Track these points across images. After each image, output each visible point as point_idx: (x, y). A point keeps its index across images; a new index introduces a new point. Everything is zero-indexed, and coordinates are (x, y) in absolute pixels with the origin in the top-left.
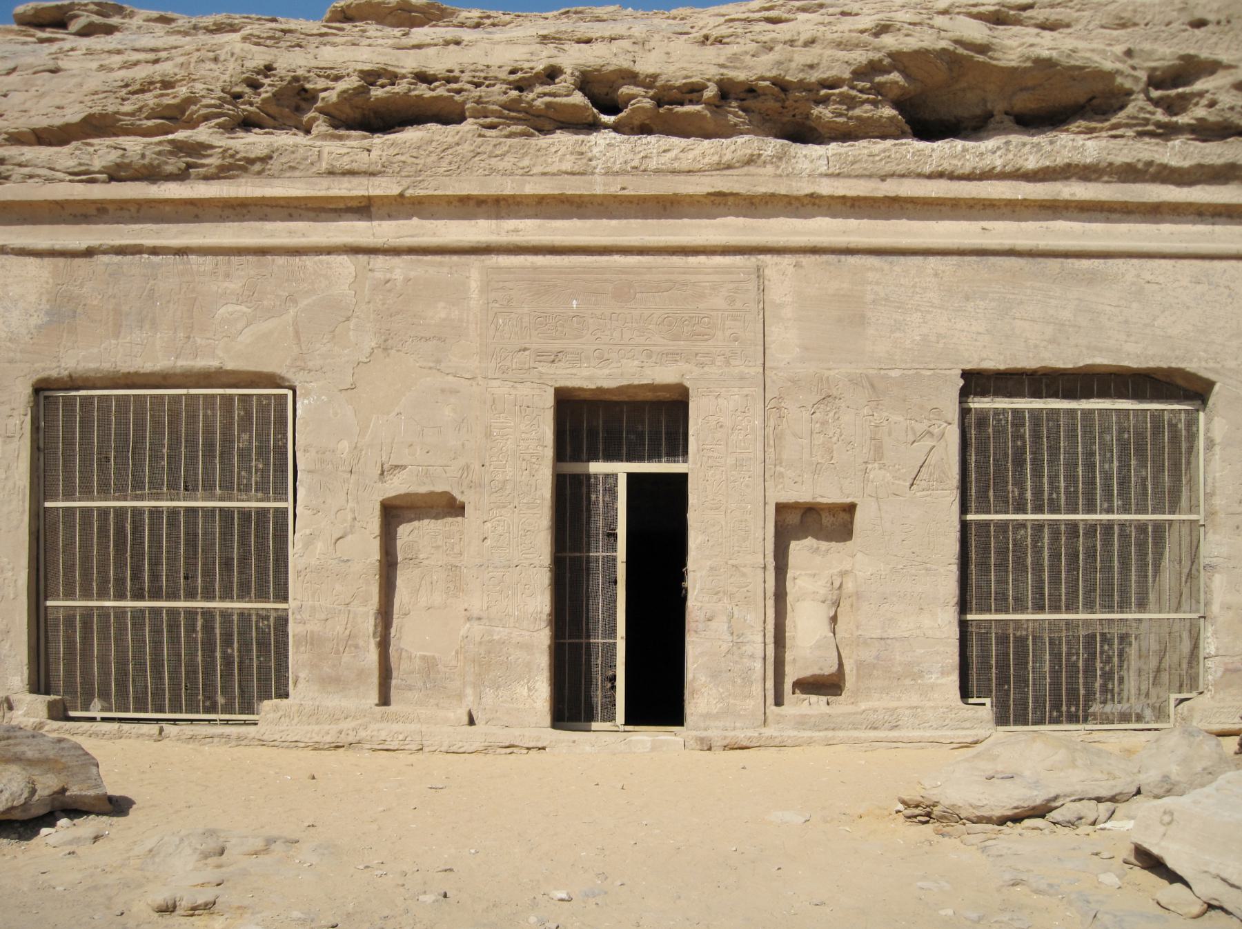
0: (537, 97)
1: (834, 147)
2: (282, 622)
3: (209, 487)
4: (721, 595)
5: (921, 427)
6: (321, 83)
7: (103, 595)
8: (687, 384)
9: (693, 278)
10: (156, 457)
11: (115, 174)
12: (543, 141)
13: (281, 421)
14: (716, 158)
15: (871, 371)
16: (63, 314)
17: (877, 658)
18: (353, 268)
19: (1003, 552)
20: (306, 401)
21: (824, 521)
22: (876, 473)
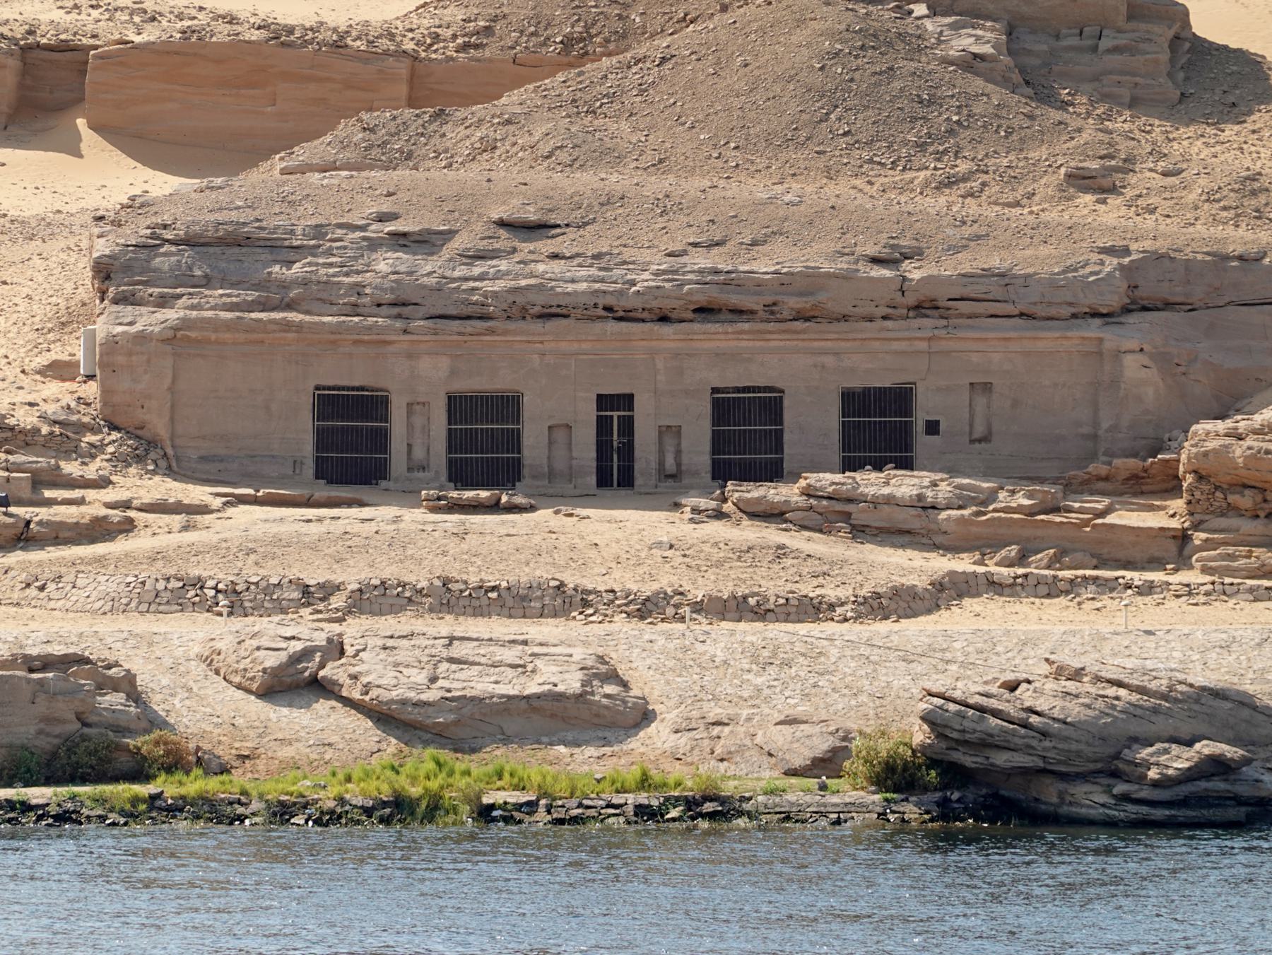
0: (592, 312)
2: (519, 459)
16: (453, 373)
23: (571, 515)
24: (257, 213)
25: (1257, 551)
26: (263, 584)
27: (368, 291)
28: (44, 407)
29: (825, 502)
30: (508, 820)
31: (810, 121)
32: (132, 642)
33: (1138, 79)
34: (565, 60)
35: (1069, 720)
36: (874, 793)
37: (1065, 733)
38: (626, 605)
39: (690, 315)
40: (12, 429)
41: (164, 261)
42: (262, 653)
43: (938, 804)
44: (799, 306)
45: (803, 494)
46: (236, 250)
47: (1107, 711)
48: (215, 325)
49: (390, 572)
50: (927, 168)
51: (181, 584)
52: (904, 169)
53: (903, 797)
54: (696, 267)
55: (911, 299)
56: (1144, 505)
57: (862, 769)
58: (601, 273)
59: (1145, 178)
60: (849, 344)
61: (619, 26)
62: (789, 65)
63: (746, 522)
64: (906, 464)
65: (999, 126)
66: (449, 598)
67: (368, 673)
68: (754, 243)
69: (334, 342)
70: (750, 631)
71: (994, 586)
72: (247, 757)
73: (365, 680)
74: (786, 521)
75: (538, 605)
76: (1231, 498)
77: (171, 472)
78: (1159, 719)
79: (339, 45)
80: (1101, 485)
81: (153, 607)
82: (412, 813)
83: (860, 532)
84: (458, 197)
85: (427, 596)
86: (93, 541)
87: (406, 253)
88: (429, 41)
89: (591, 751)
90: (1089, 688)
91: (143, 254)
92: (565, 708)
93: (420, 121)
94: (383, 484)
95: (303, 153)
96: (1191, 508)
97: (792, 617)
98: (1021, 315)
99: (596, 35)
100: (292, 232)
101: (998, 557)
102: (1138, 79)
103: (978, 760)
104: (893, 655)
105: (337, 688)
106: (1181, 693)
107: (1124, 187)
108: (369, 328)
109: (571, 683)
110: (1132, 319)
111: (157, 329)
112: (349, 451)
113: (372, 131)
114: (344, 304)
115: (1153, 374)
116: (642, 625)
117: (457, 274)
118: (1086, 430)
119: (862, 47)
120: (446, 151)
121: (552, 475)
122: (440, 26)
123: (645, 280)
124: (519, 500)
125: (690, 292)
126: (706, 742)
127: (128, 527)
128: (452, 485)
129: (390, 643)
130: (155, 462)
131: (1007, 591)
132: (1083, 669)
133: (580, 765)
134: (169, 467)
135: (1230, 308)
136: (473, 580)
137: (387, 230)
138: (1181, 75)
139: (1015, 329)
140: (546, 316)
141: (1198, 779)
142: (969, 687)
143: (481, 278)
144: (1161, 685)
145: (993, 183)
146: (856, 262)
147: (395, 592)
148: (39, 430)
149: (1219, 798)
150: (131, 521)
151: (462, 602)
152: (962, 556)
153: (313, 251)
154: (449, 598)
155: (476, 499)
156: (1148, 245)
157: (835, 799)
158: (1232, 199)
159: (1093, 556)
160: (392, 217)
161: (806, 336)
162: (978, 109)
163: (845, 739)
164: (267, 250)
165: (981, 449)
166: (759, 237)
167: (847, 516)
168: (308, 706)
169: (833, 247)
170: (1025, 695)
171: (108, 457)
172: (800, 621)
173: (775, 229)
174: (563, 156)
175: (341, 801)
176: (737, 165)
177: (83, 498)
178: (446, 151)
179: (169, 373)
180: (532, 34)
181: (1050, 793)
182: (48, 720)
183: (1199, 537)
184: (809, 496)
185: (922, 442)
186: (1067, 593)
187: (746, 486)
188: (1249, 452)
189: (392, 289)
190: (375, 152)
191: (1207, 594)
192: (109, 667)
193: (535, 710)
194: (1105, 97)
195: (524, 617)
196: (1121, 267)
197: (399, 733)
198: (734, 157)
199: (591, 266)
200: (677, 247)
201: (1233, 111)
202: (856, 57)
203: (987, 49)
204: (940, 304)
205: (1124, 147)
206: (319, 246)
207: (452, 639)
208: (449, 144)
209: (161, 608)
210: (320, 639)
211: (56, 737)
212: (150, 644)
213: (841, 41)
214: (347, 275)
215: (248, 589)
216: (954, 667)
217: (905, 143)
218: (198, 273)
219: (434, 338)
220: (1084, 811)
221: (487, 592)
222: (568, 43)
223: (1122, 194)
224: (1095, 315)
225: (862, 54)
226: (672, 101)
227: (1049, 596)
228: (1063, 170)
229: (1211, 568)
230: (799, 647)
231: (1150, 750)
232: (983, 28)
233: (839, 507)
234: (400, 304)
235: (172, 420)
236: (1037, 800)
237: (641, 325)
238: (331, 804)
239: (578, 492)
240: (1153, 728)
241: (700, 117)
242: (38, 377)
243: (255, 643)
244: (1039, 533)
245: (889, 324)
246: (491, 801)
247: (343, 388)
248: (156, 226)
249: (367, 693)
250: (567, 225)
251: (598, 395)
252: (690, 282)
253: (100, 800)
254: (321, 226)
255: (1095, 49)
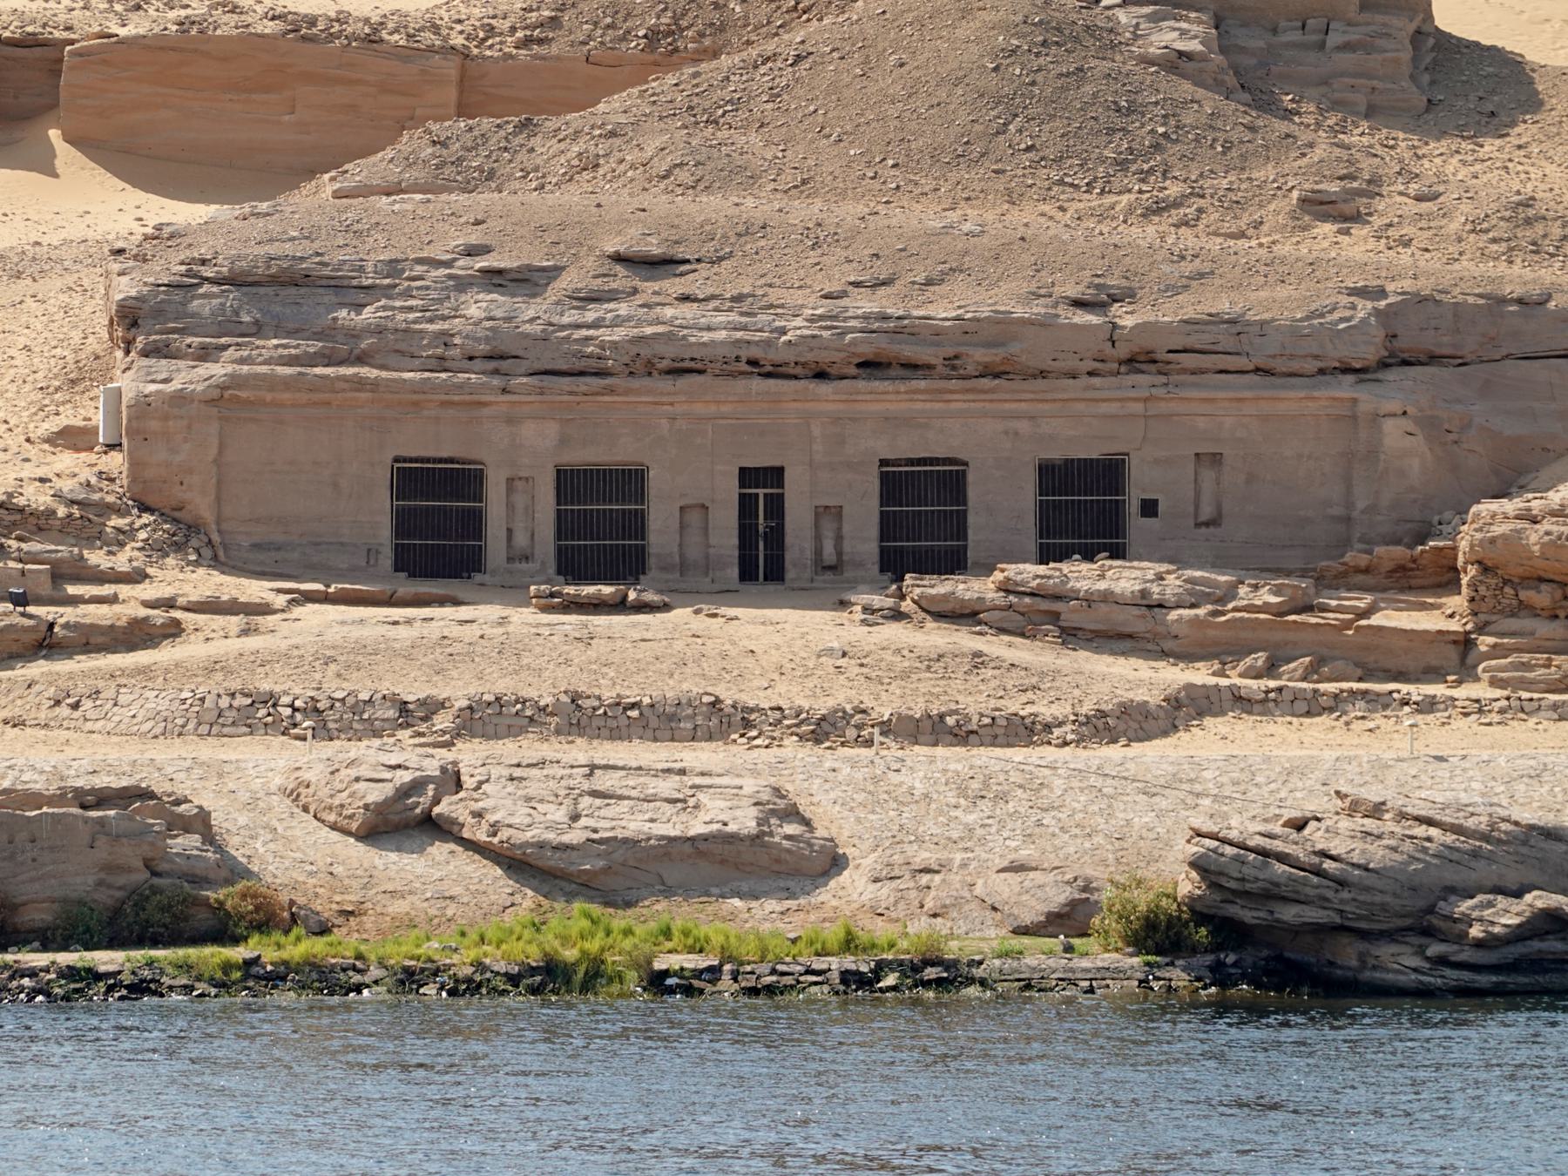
1: (836, 383)
2: (643, 547)
16: (564, 441)
23: (715, 615)
24: (316, 245)
25: (1558, 660)
26: (351, 701)
27: (457, 341)
28: (59, 484)
29: (1027, 600)
30: (689, 991)
31: (984, 134)
32: (197, 772)
33: (1375, 83)
34: (650, 58)
35: (1372, 866)
36: (1131, 955)
37: (1368, 882)
38: (796, 725)
39: (853, 371)
40: (21, 510)
41: (205, 304)
42: (362, 785)
43: (1212, 969)
44: (987, 359)
45: (999, 589)
46: (293, 290)
47: (1418, 855)
48: (271, 382)
49: (501, 684)
50: (1129, 191)
51: (249, 701)
52: (1103, 191)
53: (1167, 960)
54: (860, 312)
55: (1123, 351)
56: (1415, 603)
57: (1111, 923)
58: (744, 319)
59: (1393, 204)
60: (1046, 406)
61: (715, 17)
62: (955, 65)
63: (930, 624)
64: (1118, 553)
65: (1214, 140)
66: (579, 717)
67: (495, 809)
68: (929, 282)
69: (416, 404)
70: (952, 758)
71: (1241, 702)
72: (352, 913)
73: (492, 818)
74: (979, 623)
75: (689, 726)
76: (1523, 595)
77: (217, 563)
78: (1480, 865)
79: (372, 40)
80: (1360, 578)
81: (215, 730)
82: (568, 982)
83: (1071, 636)
84: (562, 226)
85: (552, 714)
86: (132, 648)
87: (502, 294)
88: (481, 35)
89: (772, 905)
90: (1390, 826)
91: (178, 296)
92: (739, 852)
93: (502, 133)
94: (478, 577)
95: (359, 171)
96: (1475, 606)
97: (1000, 740)
98: (1257, 370)
99: (688, 28)
100: (361, 269)
101: (1242, 667)
102: (1375, 83)
103: (1261, 914)
104: (1130, 787)
105: (455, 829)
106: (1506, 833)
107: (1370, 214)
108: (460, 387)
109: (744, 821)
110: (1392, 375)
111: (200, 388)
112: (435, 537)
113: (444, 144)
114: (428, 357)
115: (1418, 443)
116: (818, 750)
117: (566, 320)
118: (1337, 511)
119: (1044, 43)
120: (536, 169)
121: (684, 567)
122: (494, 17)
123: (797, 328)
124: (650, 597)
125: (853, 342)
126: (913, 894)
127: (173, 631)
128: (561, 578)
129: (517, 772)
130: (197, 551)
131: (1257, 708)
132: (1383, 803)
133: (758, 921)
134: (215, 557)
135: (1507, 362)
136: (609, 695)
137: (477, 266)
138: (1426, 78)
139: (1250, 388)
140: (676, 372)
141: (1530, 938)
142: (1243, 825)
143: (596, 325)
144: (1479, 822)
145: (1211, 210)
146: (1055, 305)
147: (514, 710)
148: (54, 512)
149: (1555, 961)
150: (177, 623)
151: (596, 722)
152: (1197, 665)
153: (387, 291)
154: (579, 717)
155: (598, 595)
156: (1407, 284)
157: (1085, 963)
158: (1503, 229)
159: (1357, 665)
160: (483, 250)
161: (994, 396)
162: (1188, 119)
163: (1085, 889)
164: (331, 291)
165: (1207, 534)
166: (935, 275)
167: (1055, 617)
168: (421, 851)
169: (1026, 288)
170: (1315, 835)
171: (140, 544)
172: (1009, 745)
173: (954, 265)
174: (683, 176)
175: (479, 966)
176: (898, 187)
177: (116, 596)
178: (536, 169)
179: (215, 441)
180: (608, 27)
181: (1348, 954)
182: (110, 868)
183: (1485, 642)
184: (1008, 591)
185: (1137, 525)
186: (1331, 710)
187: (927, 580)
188: (1547, 538)
189: (487, 339)
190: (448, 171)
191: (1502, 711)
192: (178, 803)
193: (701, 854)
194: (1336, 105)
195: (673, 740)
196: (1377, 312)
197: (535, 882)
198: (894, 178)
199: (730, 310)
200: (834, 287)
201: (1492, 122)
202: (1038, 55)
203: (1194, 46)
204: (1158, 357)
205: (1367, 165)
206: (395, 286)
207: (593, 768)
208: (539, 161)
209: (226, 730)
210: (432, 768)
211: (120, 888)
212: (220, 776)
213: (1017, 35)
214: (431, 321)
215: (332, 707)
216: (1206, 802)
217: (1102, 160)
218: (246, 318)
219: (539, 398)
220: (1390, 976)
221: (625, 709)
222: (653, 37)
223: (1369, 223)
224: (1347, 370)
225: (1044, 50)
226: (812, 108)
227: (1308, 714)
228: (1295, 194)
229: (1502, 680)
230: (1015, 777)
231: (1470, 902)
232: (1187, 19)
233: (1045, 605)
234: (498, 357)
235: (218, 499)
236: (1331, 963)
237: (793, 383)
238: (469, 970)
239: (717, 587)
240: (1474, 875)
241: (848, 128)
242: (46, 446)
243: (353, 773)
244: (1291, 636)
245: (1096, 381)
246: (664, 967)
247: (428, 460)
248: (193, 261)
249: (495, 834)
250: (698, 260)
251: (742, 470)
252: (853, 330)
253: (185, 967)
254: (397, 261)
255: (1321, 46)
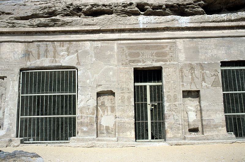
0: (128, 9)
2: (74, 119)
3: (58, 90)
4: (172, 111)
5: (213, 74)
6: (83, 7)
7: (34, 115)
8: (162, 66)
9: (162, 44)
10: (47, 84)
11: (38, 26)
12: (129, 18)
13: (74, 76)
14: (166, 20)
15: (201, 62)
16: (27, 55)
17: (207, 124)
18: (90, 44)
19: (232, 100)
20: (80, 72)
21: (192, 94)
22: (204, 84)
